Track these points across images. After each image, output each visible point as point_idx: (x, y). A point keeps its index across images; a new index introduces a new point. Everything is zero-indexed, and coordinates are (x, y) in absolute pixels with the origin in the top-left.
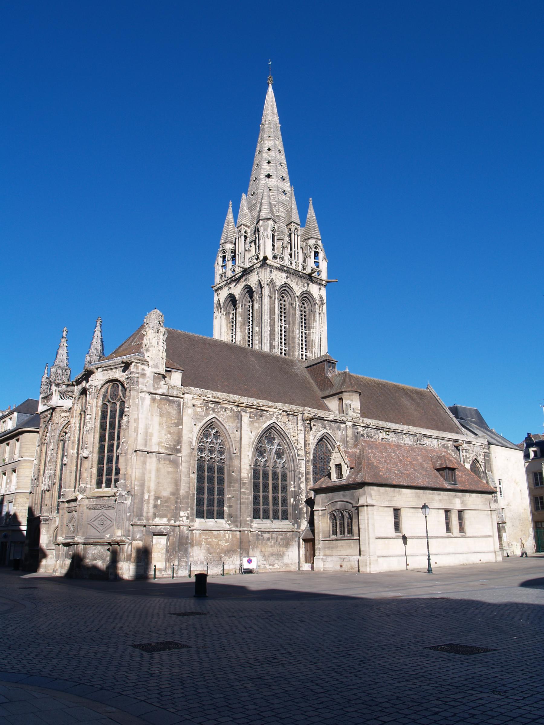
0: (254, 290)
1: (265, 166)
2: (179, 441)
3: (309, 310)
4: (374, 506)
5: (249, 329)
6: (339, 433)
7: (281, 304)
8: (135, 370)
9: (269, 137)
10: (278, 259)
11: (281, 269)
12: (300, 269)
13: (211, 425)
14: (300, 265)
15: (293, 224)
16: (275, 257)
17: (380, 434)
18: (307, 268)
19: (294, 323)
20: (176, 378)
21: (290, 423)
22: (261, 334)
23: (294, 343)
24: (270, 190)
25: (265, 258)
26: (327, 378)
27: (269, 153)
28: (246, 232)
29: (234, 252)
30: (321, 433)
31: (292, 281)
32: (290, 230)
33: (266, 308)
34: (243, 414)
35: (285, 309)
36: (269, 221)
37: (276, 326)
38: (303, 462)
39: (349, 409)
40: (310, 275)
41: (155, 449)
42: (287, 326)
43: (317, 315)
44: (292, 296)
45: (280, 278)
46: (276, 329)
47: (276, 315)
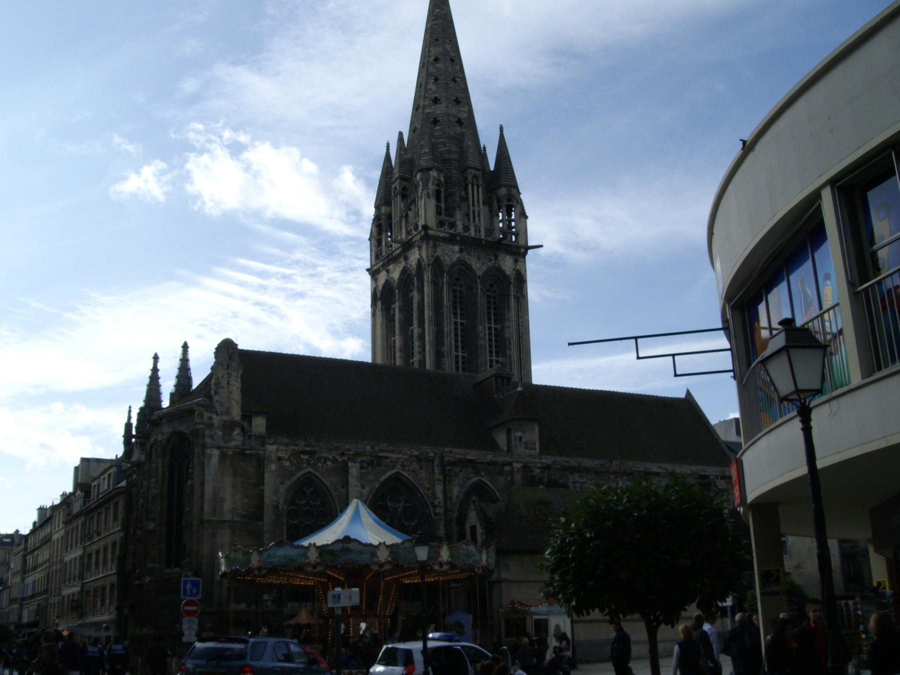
1: (432, 86)
2: (261, 505)
4: (512, 581)
6: (502, 479)
7: (455, 291)
8: (198, 421)
9: (437, 40)
10: (446, 227)
12: (483, 235)
13: (309, 480)
14: (482, 229)
16: (441, 224)
17: (571, 477)
20: (259, 424)
21: (423, 471)
22: (422, 337)
27: (437, 65)
28: (404, 189)
29: (389, 217)
30: (471, 482)
31: (470, 255)
32: (466, 179)
34: (350, 464)
35: (461, 298)
38: (442, 523)
39: (518, 443)
41: (228, 517)
43: (512, 301)
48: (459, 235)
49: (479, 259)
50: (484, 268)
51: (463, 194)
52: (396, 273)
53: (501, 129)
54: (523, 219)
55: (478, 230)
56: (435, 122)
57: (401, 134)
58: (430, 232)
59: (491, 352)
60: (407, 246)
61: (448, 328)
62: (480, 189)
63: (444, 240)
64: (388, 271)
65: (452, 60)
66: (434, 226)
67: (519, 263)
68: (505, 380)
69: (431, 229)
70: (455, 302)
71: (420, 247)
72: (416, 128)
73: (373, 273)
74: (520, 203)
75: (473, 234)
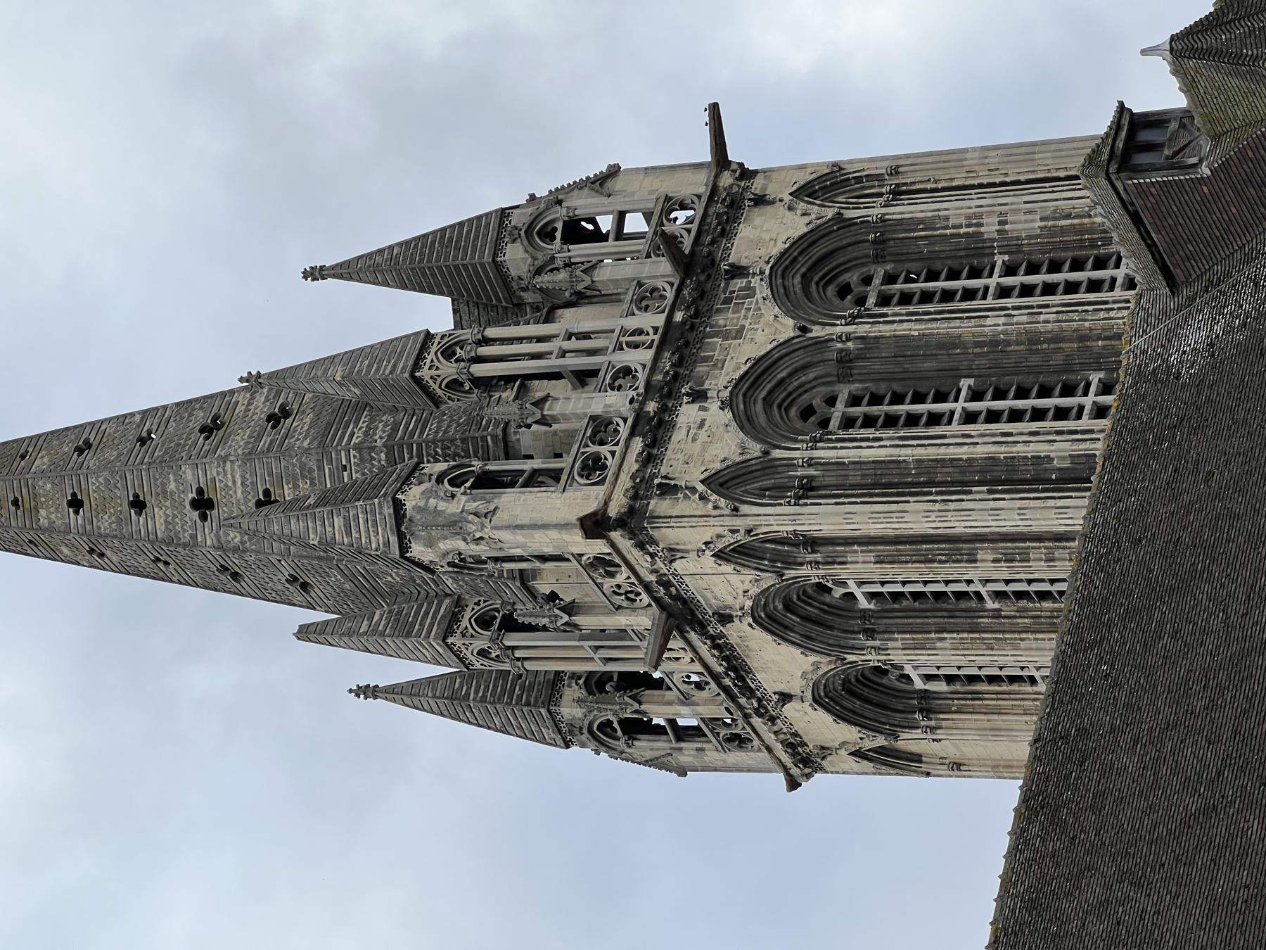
0: (769, 580)
1: (157, 518)
3: (879, 259)
5: (999, 595)
7: (848, 423)
11: (654, 430)
12: (653, 320)
14: (632, 323)
15: (425, 373)
16: (593, 467)
18: (649, 283)
19: (949, 344)
23: (1057, 338)
24: (267, 493)
25: (594, 525)
26: (1222, 171)
28: (484, 622)
29: (596, 684)
32: (454, 385)
33: (866, 518)
35: (876, 400)
36: (409, 506)
37: (963, 452)
40: (686, 264)
42: (965, 384)
43: (904, 210)
44: (798, 359)
45: (703, 434)
46: (982, 450)
47: (906, 454)
48: (638, 404)
49: (739, 333)
50: (770, 310)
51: (509, 394)
52: (781, 665)
53: (315, 274)
54: (617, 184)
55: (633, 340)
56: (266, 501)
57: (305, 633)
58: (613, 512)
59: (1094, 286)
60: (681, 614)
61: (983, 443)
62: (491, 332)
63: (648, 459)
64: (785, 698)
65: (84, 448)
66: (600, 491)
67: (772, 192)
68: (1145, 136)
69: (606, 503)
70: (891, 421)
71: (673, 553)
72: (293, 580)
73: (803, 761)
74: (556, 199)
75: (647, 355)
